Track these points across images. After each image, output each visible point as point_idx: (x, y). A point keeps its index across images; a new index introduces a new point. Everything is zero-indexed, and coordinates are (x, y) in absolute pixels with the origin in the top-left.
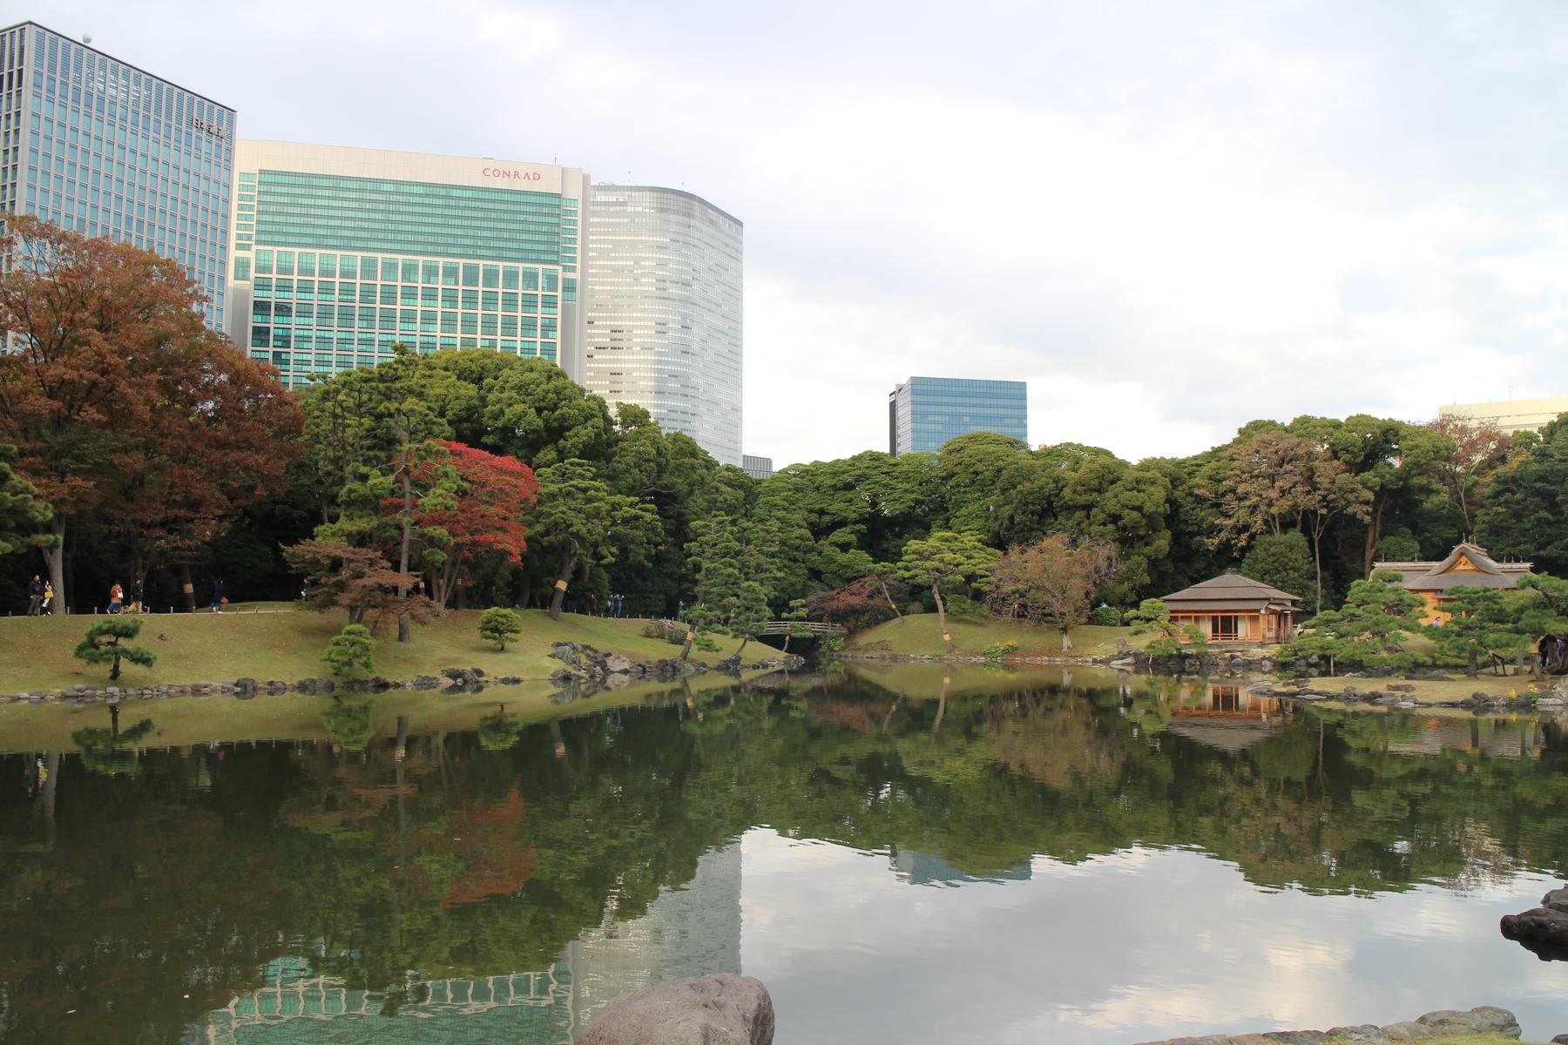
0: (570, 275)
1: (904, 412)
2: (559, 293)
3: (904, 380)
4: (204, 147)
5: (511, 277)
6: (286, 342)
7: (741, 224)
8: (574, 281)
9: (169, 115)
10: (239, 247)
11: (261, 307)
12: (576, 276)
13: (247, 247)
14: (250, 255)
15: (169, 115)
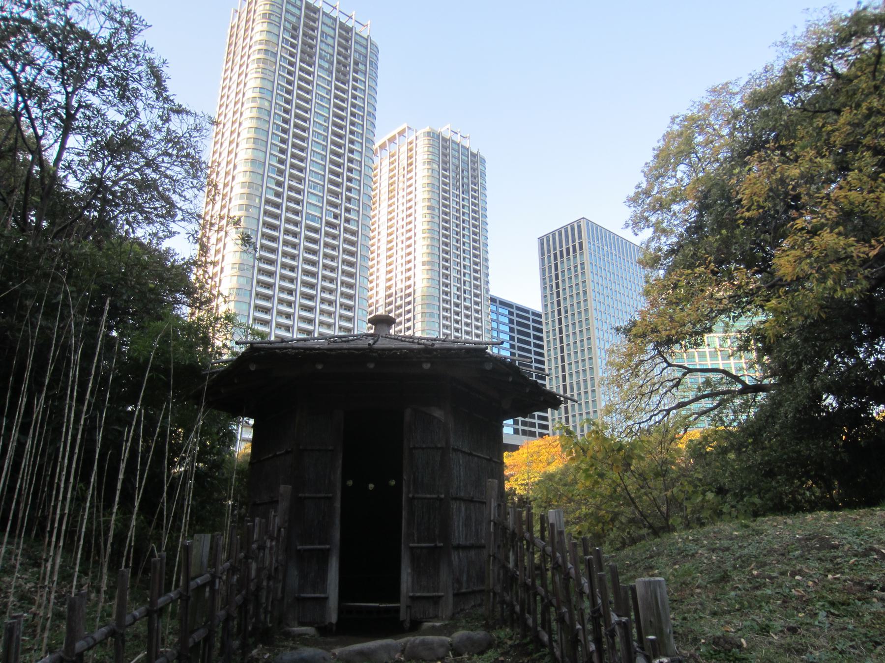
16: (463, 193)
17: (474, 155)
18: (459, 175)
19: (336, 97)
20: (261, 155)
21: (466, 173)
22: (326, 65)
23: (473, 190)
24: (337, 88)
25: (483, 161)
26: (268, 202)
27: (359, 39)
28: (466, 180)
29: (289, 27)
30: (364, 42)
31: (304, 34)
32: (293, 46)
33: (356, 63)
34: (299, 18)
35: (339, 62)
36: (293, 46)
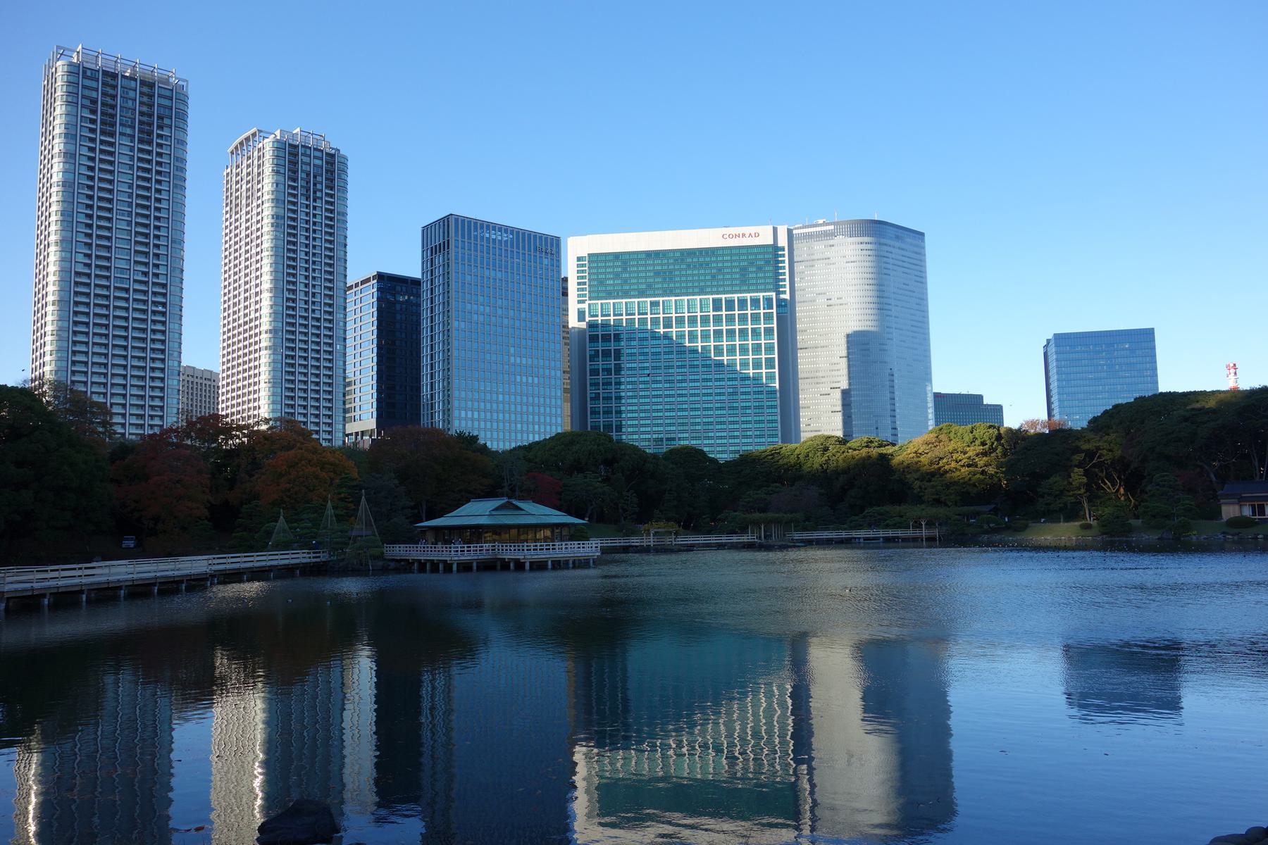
0: (782, 296)
1: (1052, 358)
2: (774, 311)
3: (1050, 337)
4: (545, 262)
5: (743, 303)
6: (618, 357)
7: (922, 234)
8: (785, 300)
9: (524, 248)
10: (579, 302)
11: (594, 339)
12: (787, 296)
13: (583, 302)
14: (585, 306)
15: (524, 248)
16: (315, 200)
17: (333, 156)
18: (311, 183)
19: (140, 159)
20: (69, 234)
21: (319, 179)
22: (128, 131)
23: (327, 194)
24: (140, 150)
25: (344, 163)
26: (78, 274)
27: (163, 92)
28: (319, 186)
29: (87, 102)
30: (168, 94)
31: (103, 104)
32: (93, 121)
33: (160, 118)
34: (97, 90)
35: (141, 123)
36: (93, 121)
